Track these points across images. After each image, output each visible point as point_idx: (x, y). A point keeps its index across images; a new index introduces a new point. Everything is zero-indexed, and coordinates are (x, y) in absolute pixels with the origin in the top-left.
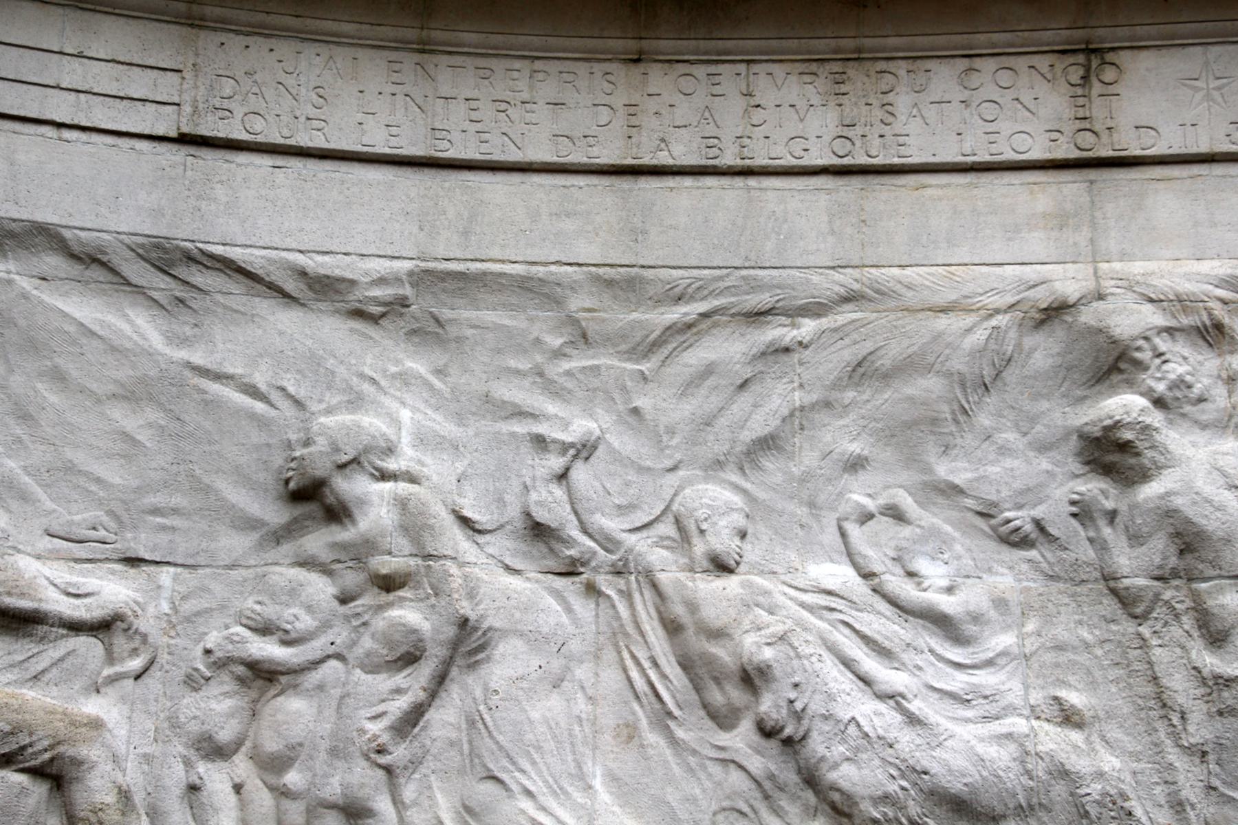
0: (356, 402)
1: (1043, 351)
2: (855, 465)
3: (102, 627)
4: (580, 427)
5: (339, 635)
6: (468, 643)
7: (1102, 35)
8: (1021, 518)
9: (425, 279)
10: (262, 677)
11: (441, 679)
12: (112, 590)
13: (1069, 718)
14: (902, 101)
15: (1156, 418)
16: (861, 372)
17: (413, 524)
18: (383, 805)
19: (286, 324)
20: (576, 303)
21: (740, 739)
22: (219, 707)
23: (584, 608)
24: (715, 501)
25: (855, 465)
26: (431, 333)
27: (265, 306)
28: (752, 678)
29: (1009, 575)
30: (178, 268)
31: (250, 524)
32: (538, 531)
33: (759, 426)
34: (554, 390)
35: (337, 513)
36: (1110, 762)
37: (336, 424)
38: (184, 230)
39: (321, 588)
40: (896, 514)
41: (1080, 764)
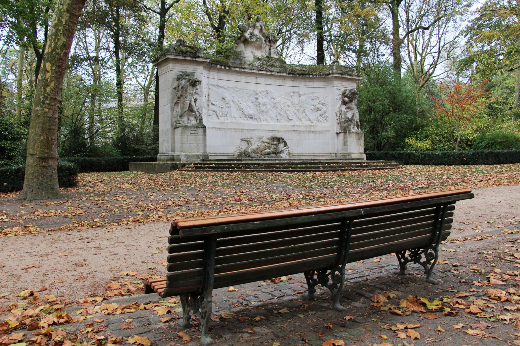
1: (254, 93)
24: (240, 100)
26: (228, 90)
30: (218, 86)
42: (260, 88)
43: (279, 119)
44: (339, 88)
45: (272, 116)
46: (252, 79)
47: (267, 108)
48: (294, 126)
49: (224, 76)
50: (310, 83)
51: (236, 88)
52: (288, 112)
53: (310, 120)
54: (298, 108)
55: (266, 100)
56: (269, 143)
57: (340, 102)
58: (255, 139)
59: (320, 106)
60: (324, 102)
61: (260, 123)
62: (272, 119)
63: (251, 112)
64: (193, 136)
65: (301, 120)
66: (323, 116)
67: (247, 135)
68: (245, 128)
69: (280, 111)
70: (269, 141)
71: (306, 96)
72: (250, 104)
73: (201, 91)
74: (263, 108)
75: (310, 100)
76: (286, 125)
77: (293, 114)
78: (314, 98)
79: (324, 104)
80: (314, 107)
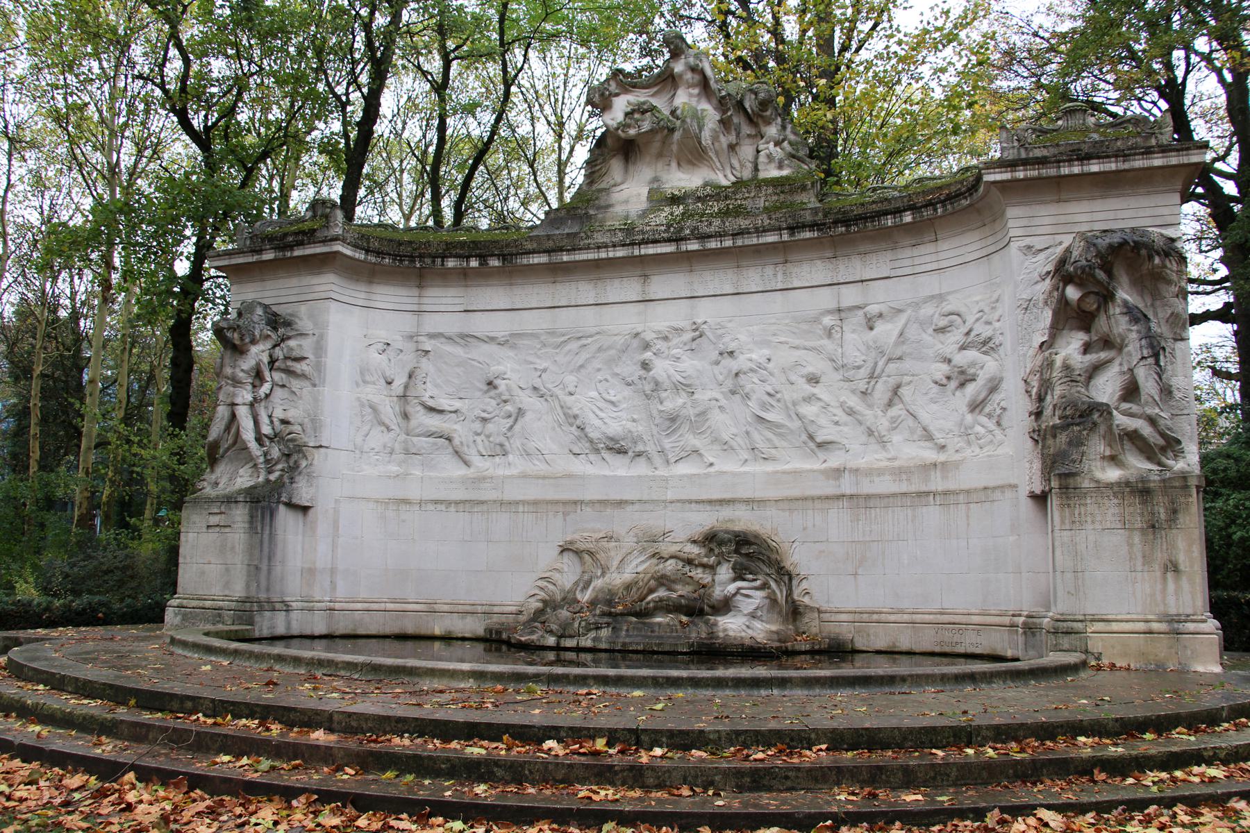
0: (499, 364)
1: (635, 343)
2: (599, 370)
3: (455, 412)
4: (544, 365)
5: (497, 412)
6: (521, 412)
7: (648, 272)
8: (629, 380)
9: (512, 335)
10: (484, 420)
11: (516, 420)
12: (457, 404)
13: (634, 421)
14: (608, 288)
15: (654, 357)
16: (600, 350)
17: (509, 389)
18: (507, 444)
19: (485, 347)
20: (543, 338)
21: (574, 429)
22: (477, 426)
23: (545, 404)
25: (599, 370)
27: (481, 344)
28: (575, 417)
29: (627, 391)
30: (466, 338)
31: (481, 390)
32: (535, 388)
33: (580, 363)
34: (539, 357)
35: (495, 388)
36: (640, 428)
37: (496, 369)
38: (466, 331)
39: (494, 403)
40: (606, 380)
41: (634, 430)
42: (661, 318)
43: (760, 445)
44: (1038, 243)
45: (726, 437)
46: (624, 288)
47: (695, 403)
48: (838, 472)
49: (493, 295)
50: (922, 249)
51: (552, 333)
52: (809, 410)
53: (928, 436)
54: (862, 386)
55: (690, 364)
56: (689, 562)
57: (1048, 315)
58: (629, 542)
59: (972, 354)
60: (986, 332)
62: (727, 447)
63: (615, 428)
64: (213, 536)
65: (883, 443)
67: (587, 528)
68: (588, 497)
69: (764, 406)
70: (694, 550)
71: (903, 319)
72: (617, 392)
73: (319, 367)
74: (673, 402)
75: (928, 337)
76: (795, 472)
77: (841, 416)
78: (943, 322)
79: (987, 345)
80: (945, 368)
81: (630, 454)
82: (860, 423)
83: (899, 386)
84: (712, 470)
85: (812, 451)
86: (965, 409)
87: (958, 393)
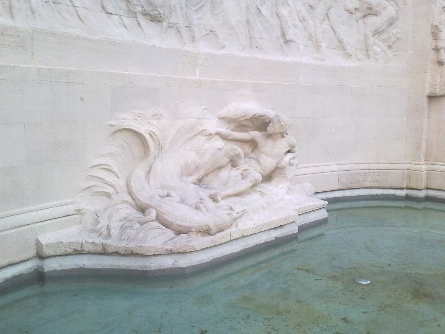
53: (341, 45)
61: (188, 47)
65: (318, 47)
66: (384, 36)
77: (298, 23)
81: (165, 24)
82: (306, 30)
83: (330, 7)
84: (223, 52)
85: (281, 46)
86: (370, 34)
87: (361, 21)
